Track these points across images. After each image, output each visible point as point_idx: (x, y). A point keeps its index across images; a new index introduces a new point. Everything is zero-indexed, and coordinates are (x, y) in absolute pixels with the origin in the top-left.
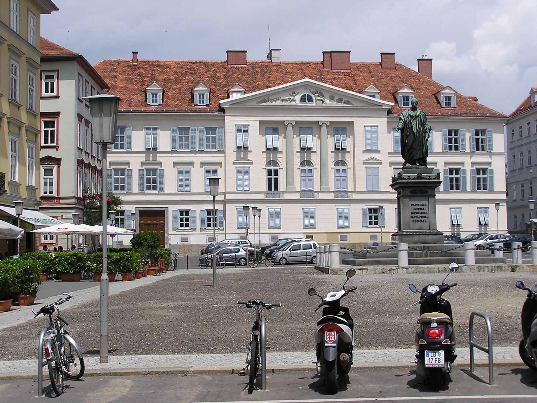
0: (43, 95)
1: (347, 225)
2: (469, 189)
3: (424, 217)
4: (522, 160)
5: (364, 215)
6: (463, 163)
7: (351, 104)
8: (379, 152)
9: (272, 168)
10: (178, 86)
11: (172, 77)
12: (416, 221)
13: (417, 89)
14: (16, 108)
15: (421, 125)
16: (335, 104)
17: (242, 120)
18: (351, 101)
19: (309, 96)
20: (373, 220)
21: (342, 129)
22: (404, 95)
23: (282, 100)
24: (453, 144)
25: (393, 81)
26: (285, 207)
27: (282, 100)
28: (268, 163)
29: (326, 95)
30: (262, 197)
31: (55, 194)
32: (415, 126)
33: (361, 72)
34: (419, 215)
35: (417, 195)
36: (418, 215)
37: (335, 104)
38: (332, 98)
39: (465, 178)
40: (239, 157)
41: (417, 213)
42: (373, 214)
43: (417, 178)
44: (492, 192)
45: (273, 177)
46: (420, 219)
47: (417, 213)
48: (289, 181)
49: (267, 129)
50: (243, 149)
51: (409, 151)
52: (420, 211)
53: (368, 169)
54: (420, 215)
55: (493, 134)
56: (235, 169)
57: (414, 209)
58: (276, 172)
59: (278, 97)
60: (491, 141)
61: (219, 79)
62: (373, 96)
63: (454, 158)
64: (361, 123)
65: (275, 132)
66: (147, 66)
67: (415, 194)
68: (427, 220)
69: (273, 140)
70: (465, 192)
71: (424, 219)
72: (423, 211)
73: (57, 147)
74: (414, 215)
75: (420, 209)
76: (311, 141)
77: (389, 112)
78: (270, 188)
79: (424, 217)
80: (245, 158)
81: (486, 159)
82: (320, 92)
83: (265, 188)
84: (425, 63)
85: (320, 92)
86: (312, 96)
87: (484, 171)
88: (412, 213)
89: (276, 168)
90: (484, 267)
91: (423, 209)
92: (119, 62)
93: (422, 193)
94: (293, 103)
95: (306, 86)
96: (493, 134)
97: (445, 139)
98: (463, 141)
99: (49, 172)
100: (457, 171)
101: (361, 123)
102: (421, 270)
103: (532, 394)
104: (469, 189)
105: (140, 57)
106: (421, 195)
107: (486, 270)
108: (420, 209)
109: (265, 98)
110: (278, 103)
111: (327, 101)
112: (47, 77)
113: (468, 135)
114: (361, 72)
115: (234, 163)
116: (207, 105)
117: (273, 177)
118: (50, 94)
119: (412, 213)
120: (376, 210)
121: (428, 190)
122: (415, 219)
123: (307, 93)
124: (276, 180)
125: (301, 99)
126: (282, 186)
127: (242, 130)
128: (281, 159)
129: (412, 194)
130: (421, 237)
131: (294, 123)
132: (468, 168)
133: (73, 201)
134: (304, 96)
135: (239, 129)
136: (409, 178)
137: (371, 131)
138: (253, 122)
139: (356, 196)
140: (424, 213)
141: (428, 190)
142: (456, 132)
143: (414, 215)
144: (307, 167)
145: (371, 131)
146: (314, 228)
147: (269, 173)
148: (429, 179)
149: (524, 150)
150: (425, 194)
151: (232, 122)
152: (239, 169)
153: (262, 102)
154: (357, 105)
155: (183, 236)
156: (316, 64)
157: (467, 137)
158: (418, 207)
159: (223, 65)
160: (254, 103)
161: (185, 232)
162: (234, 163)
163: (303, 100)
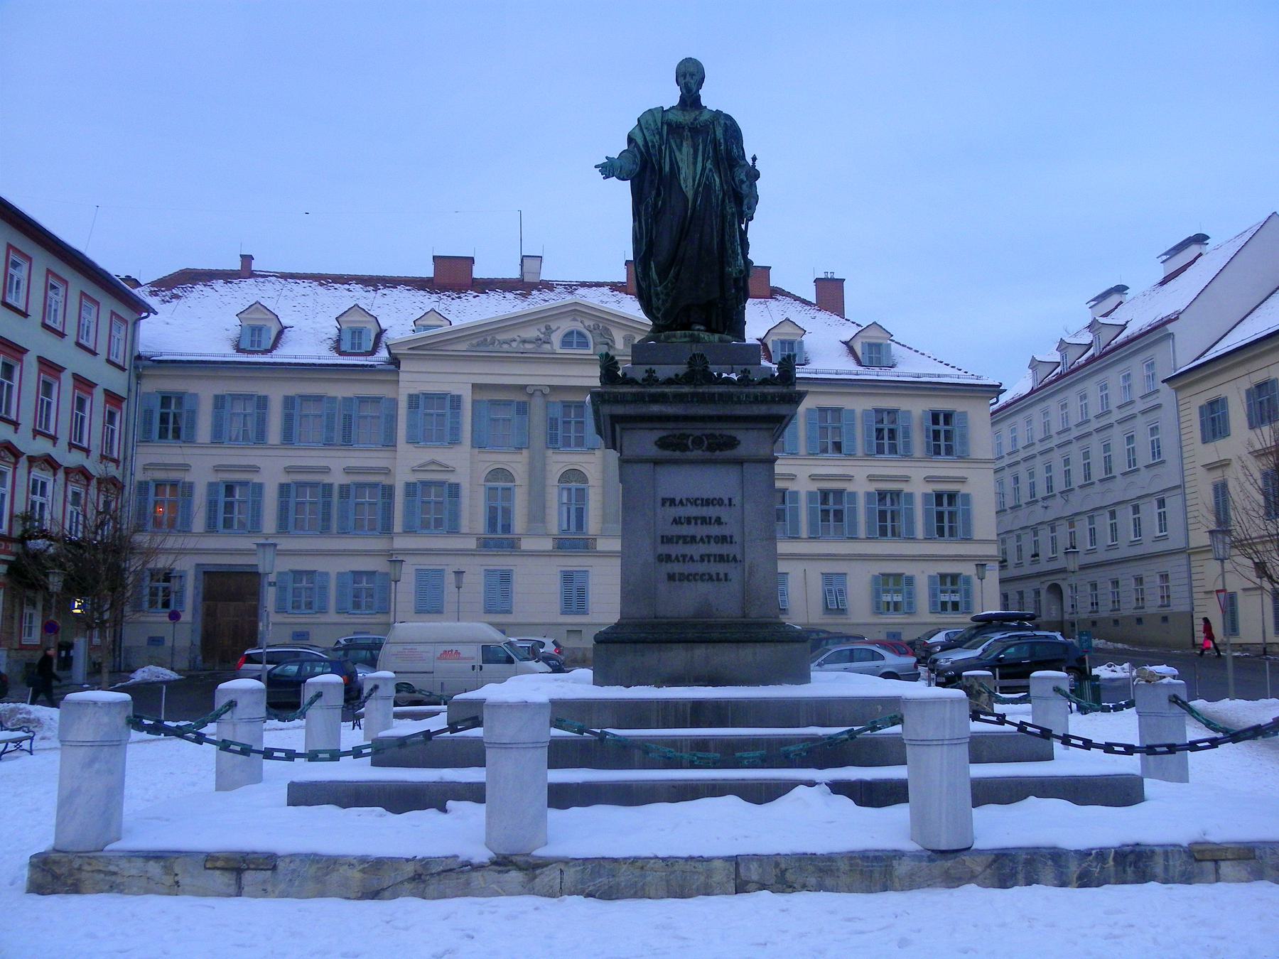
3: (722, 558)
4: (1017, 490)
15: (717, 164)
19: (580, 334)
34: (696, 550)
41: (693, 539)
43: (689, 378)
44: (968, 539)
46: (702, 568)
48: (537, 514)
51: (663, 274)
54: (703, 549)
57: (677, 521)
67: (677, 454)
68: (733, 571)
70: (911, 538)
71: (721, 568)
72: (715, 530)
74: (675, 550)
75: (705, 521)
79: (722, 558)
83: (481, 526)
87: (952, 497)
88: (666, 540)
91: (719, 521)
93: (711, 448)
94: (547, 347)
106: (708, 455)
108: (705, 521)
121: (740, 435)
122: (677, 568)
126: (519, 525)
129: (668, 454)
130: (700, 652)
131: (547, 391)
134: (570, 333)
136: (651, 379)
140: (723, 539)
141: (740, 435)
143: (675, 550)
149: (1022, 470)
150: (728, 453)
155: (298, 629)
160: (463, 346)
163: (566, 342)
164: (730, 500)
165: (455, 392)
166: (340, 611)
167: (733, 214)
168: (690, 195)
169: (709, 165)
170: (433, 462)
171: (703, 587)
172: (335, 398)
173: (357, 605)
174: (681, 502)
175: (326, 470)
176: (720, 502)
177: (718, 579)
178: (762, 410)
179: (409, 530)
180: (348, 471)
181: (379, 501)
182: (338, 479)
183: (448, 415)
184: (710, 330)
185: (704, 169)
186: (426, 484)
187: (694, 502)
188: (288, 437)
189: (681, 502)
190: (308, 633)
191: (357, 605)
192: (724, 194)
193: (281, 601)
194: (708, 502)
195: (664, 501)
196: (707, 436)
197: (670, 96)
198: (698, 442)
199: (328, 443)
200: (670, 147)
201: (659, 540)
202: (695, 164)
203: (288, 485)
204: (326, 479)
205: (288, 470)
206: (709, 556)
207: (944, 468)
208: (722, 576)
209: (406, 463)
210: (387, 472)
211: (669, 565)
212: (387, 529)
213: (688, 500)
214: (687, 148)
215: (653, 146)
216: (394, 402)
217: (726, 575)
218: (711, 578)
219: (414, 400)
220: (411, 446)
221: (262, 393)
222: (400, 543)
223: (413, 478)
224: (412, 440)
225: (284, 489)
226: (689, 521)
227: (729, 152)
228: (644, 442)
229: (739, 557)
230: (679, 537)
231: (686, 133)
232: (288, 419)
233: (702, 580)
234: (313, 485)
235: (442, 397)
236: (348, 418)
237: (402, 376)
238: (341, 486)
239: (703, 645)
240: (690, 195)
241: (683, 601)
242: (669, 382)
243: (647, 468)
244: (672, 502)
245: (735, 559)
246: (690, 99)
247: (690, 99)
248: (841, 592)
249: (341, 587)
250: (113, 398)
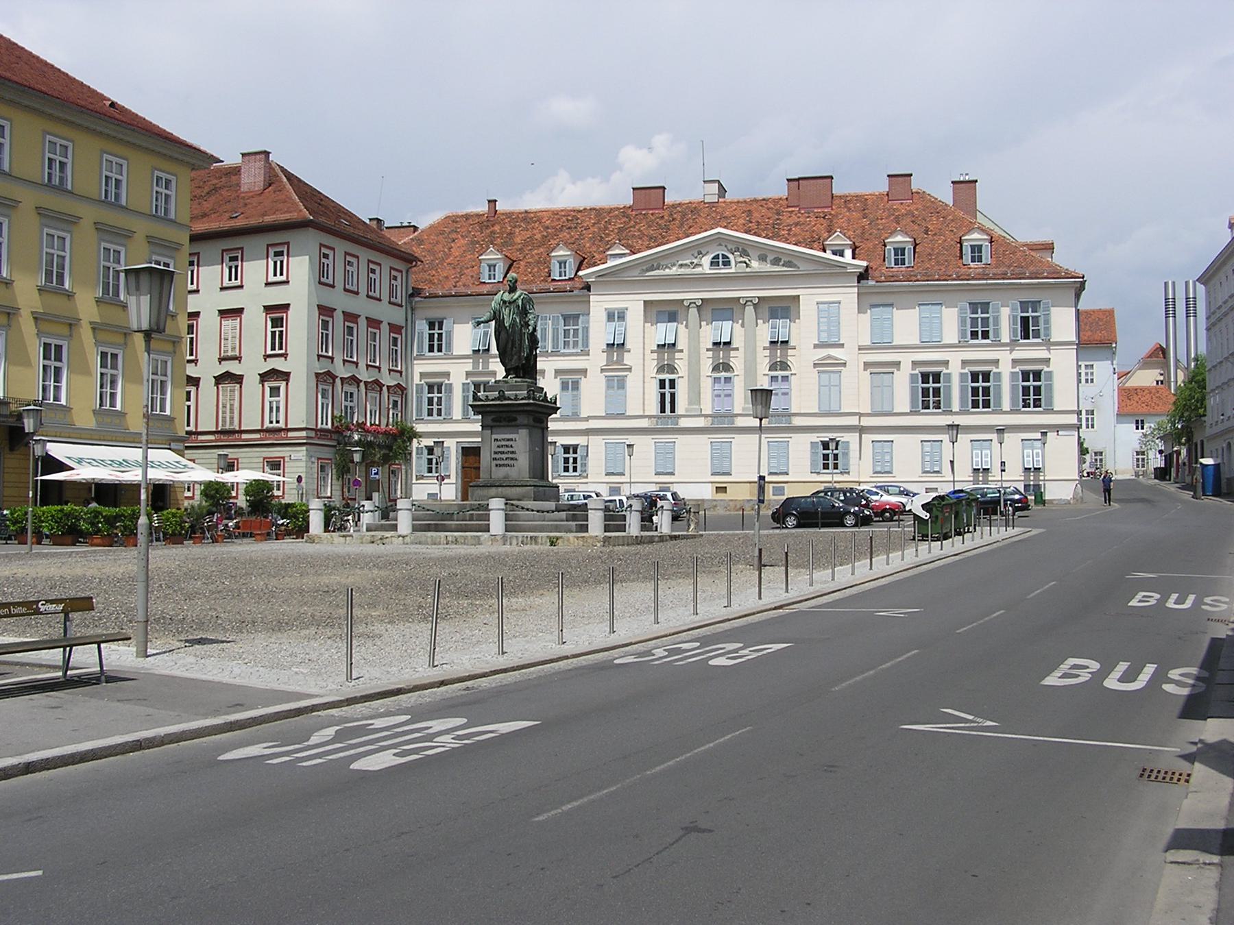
0: (270, 280)
1: (783, 469)
2: (956, 407)
5: (814, 453)
6: (996, 362)
7: (795, 266)
8: (842, 346)
9: (667, 377)
14: (120, 309)
16: (768, 267)
17: (615, 301)
18: (795, 262)
19: (724, 256)
21: (783, 309)
22: (896, 246)
23: (681, 266)
26: (681, 439)
27: (681, 266)
28: (661, 369)
29: (754, 254)
30: (644, 423)
31: (282, 425)
32: (508, 317)
33: (849, 209)
34: (504, 456)
37: (768, 267)
38: (762, 258)
39: (999, 388)
40: (609, 361)
44: (1051, 411)
45: (667, 390)
48: (695, 396)
49: (659, 313)
50: (616, 347)
52: (506, 450)
53: (823, 375)
55: (1053, 310)
56: (604, 380)
58: (672, 382)
59: (674, 261)
60: (1047, 322)
61: (608, 235)
62: (842, 254)
63: (980, 353)
64: (810, 298)
65: (672, 317)
69: (662, 332)
73: (285, 356)
76: (725, 330)
77: (863, 276)
78: (663, 410)
80: (620, 361)
81: (1041, 354)
82: (743, 250)
83: (653, 408)
85: (743, 250)
86: (730, 256)
89: (672, 376)
90: (511, 537)
92: (467, 217)
95: (719, 240)
96: (1053, 310)
98: (997, 320)
99: (275, 391)
100: (986, 376)
101: (810, 298)
102: (423, 539)
103: (205, 716)
104: (1006, 406)
105: (500, 207)
107: (514, 542)
109: (653, 264)
110: (674, 270)
111: (755, 265)
112: (232, 259)
113: (1005, 312)
114: (849, 209)
115: (602, 370)
116: (570, 279)
117: (667, 390)
118: (279, 278)
123: (720, 253)
124: (673, 396)
125: (712, 263)
126: (681, 408)
127: (617, 316)
128: (681, 364)
132: (955, 370)
133: (304, 434)
134: (717, 257)
135: (611, 316)
136: (487, 399)
137: (829, 311)
138: (633, 304)
139: (797, 422)
140: (513, 452)
142: (985, 307)
144: (724, 374)
145: (829, 311)
146: (729, 474)
147: (662, 383)
148: (516, 399)
151: (599, 304)
152: (609, 380)
153: (648, 270)
154: (804, 267)
156: (776, 201)
157: (1005, 318)
159: (624, 212)
160: (636, 272)
162: (602, 370)
163: (714, 263)
207: (1030, 352)
228: (489, 419)
250: (395, 328)
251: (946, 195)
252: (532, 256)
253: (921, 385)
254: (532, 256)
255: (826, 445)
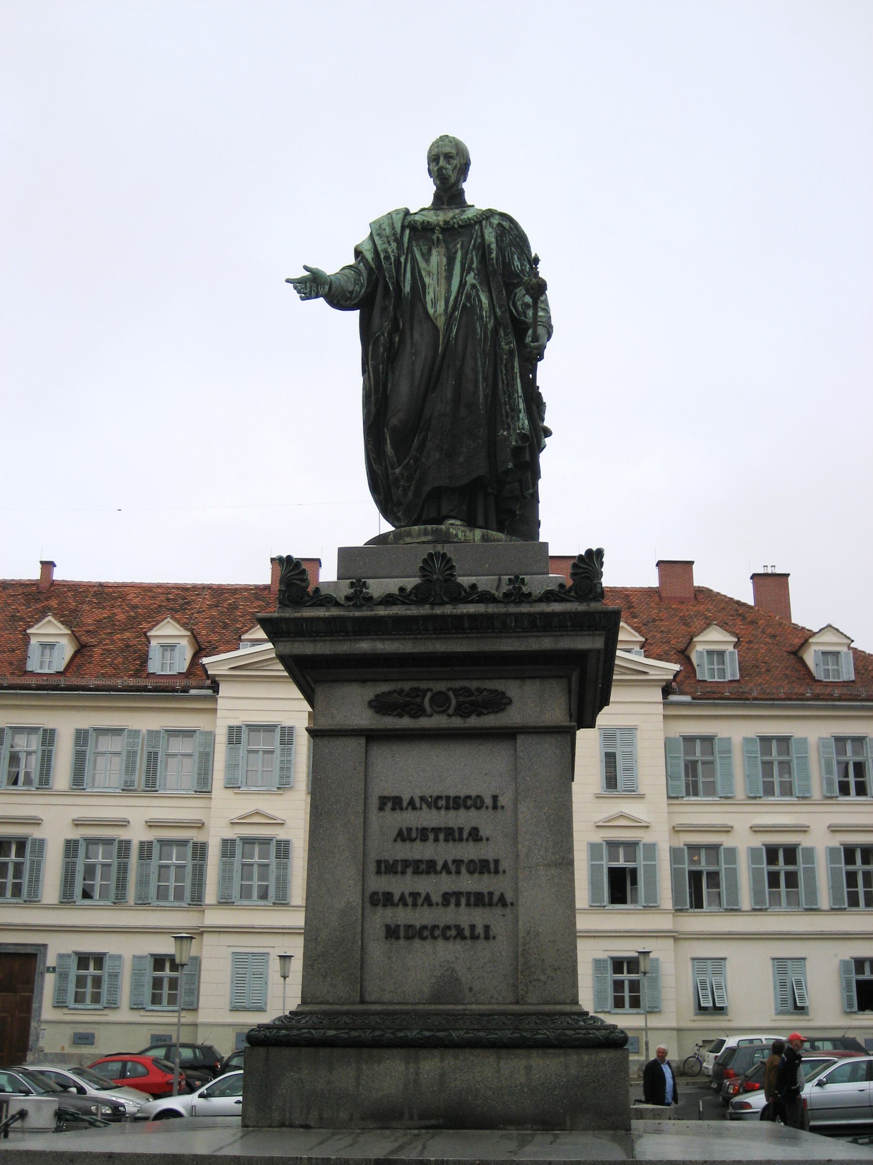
3: (479, 900)
10: (127, 634)
11: (121, 617)
12: (415, 933)
13: (750, 642)
20: (627, 994)
24: (852, 779)
25: (687, 625)
35: (424, 722)
36: (424, 885)
41: (429, 867)
42: (625, 976)
47: (429, 867)
57: (404, 836)
66: (69, 594)
67: (406, 722)
71: (478, 917)
72: (468, 851)
74: (399, 885)
75: (451, 835)
79: (479, 900)
84: (772, 585)
88: (386, 868)
91: (475, 835)
93: (462, 711)
97: (828, 765)
106: (457, 722)
108: (451, 835)
119: (386, 868)
120: (632, 964)
122: (402, 916)
130: (431, 1065)
140: (482, 867)
141: (511, 688)
143: (399, 885)
150: (489, 721)
155: (81, 1029)
158: (430, 818)
161: (85, 1016)
164: (495, 798)
165: (287, 723)
166: (136, 1007)
167: (511, 353)
168: (441, 323)
169: (471, 279)
170: (257, 813)
171: (445, 952)
172: (137, 732)
173: (156, 999)
174: (411, 802)
175: (124, 824)
176: (477, 803)
177: (474, 937)
178: (546, 643)
179: (225, 902)
180: (152, 825)
181: (189, 862)
182: (137, 834)
183: (278, 752)
184: (471, 523)
185: (462, 284)
186: (248, 841)
187: (433, 803)
188: (78, 778)
189: (411, 802)
190: (92, 1036)
191: (156, 999)
192: (498, 323)
193: (61, 991)
194: (457, 803)
195: (383, 801)
196: (455, 691)
197: (419, 194)
198: (440, 702)
199: (128, 789)
200: (414, 261)
201: (372, 867)
202: (449, 279)
203: (76, 842)
204: (123, 834)
205: (78, 823)
206: (458, 895)
208: (480, 930)
209: (222, 815)
210: (200, 826)
211: (389, 911)
212: (197, 900)
213: (422, 799)
214: (437, 258)
215: (387, 258)
216: (210, 736)
217: (487, 928)
218: (460, 935)
219: (234, 735)
220: (230, 791)
221: (50, 726)
222: (214, 918)
223: (231, 833)
224: (232, 785)
225: (71, 847)
226: (424, 834)
227: (507, 265)
229: (509, 897)
230: (406, 863)
231: (437, 235)
232: (80, 759)
233: (446, 938)
234: (108, 842)
235: (269, 728)
236: (152, 758)
237: (221, 703)
238: (142, 844)
239: (436, 1052)
240: (441, 323)
241: (407, 975)
242: (389, 600)
243: (356, 745)
244: (396, 803)
245: (502, 901)
246: (449, 192)
247: (449, 192)
248: (799, 983)
249: (137, 974)
251: (745, 594)
252: (113, 642)
253: (765, 867)
254: (113, 642)
255: (618, 964)
